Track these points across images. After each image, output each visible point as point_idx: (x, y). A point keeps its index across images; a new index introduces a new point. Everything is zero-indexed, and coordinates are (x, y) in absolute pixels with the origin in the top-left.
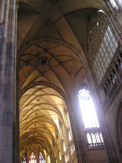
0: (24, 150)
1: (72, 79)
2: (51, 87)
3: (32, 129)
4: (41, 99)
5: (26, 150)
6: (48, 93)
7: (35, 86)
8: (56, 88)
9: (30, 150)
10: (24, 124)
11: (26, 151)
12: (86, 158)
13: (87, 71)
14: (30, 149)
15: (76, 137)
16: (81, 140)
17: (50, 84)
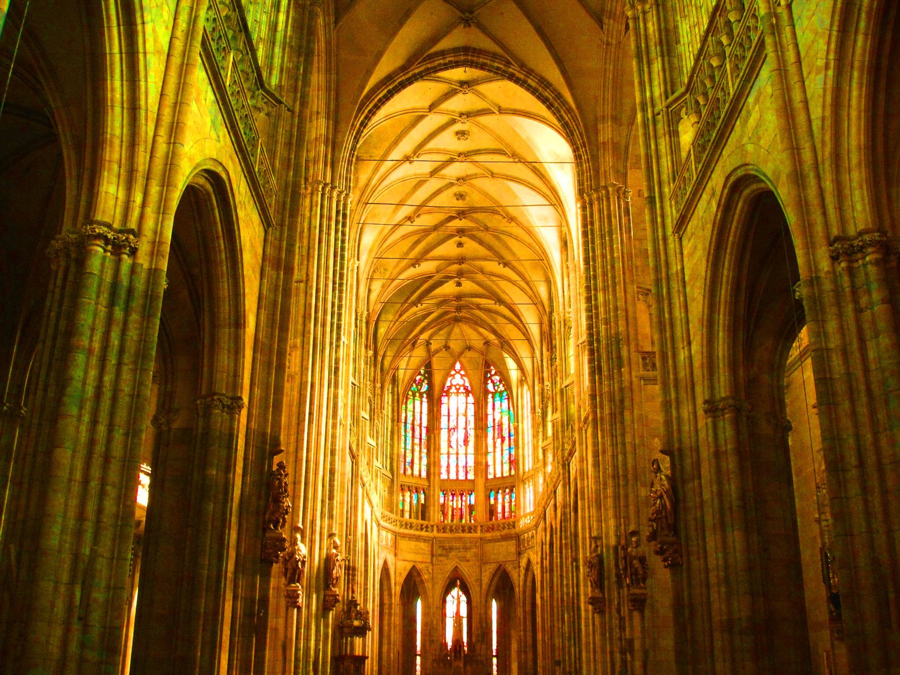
0: (420, 353)
1: (608, 44)
2: (512, 78)
3: (449, 261)
4: (474, 129)
5: (429, 351)
6: (504, 105)
7: (436, 69)
8: (533, 84)
9: (443, 353)
10: (404, 237)
11: (430, 354)
12: (627, 414)
13: (644, 13)
14: (447, 347)
15: (597, 317)
16: (617, 334)
17: (508, 64)
